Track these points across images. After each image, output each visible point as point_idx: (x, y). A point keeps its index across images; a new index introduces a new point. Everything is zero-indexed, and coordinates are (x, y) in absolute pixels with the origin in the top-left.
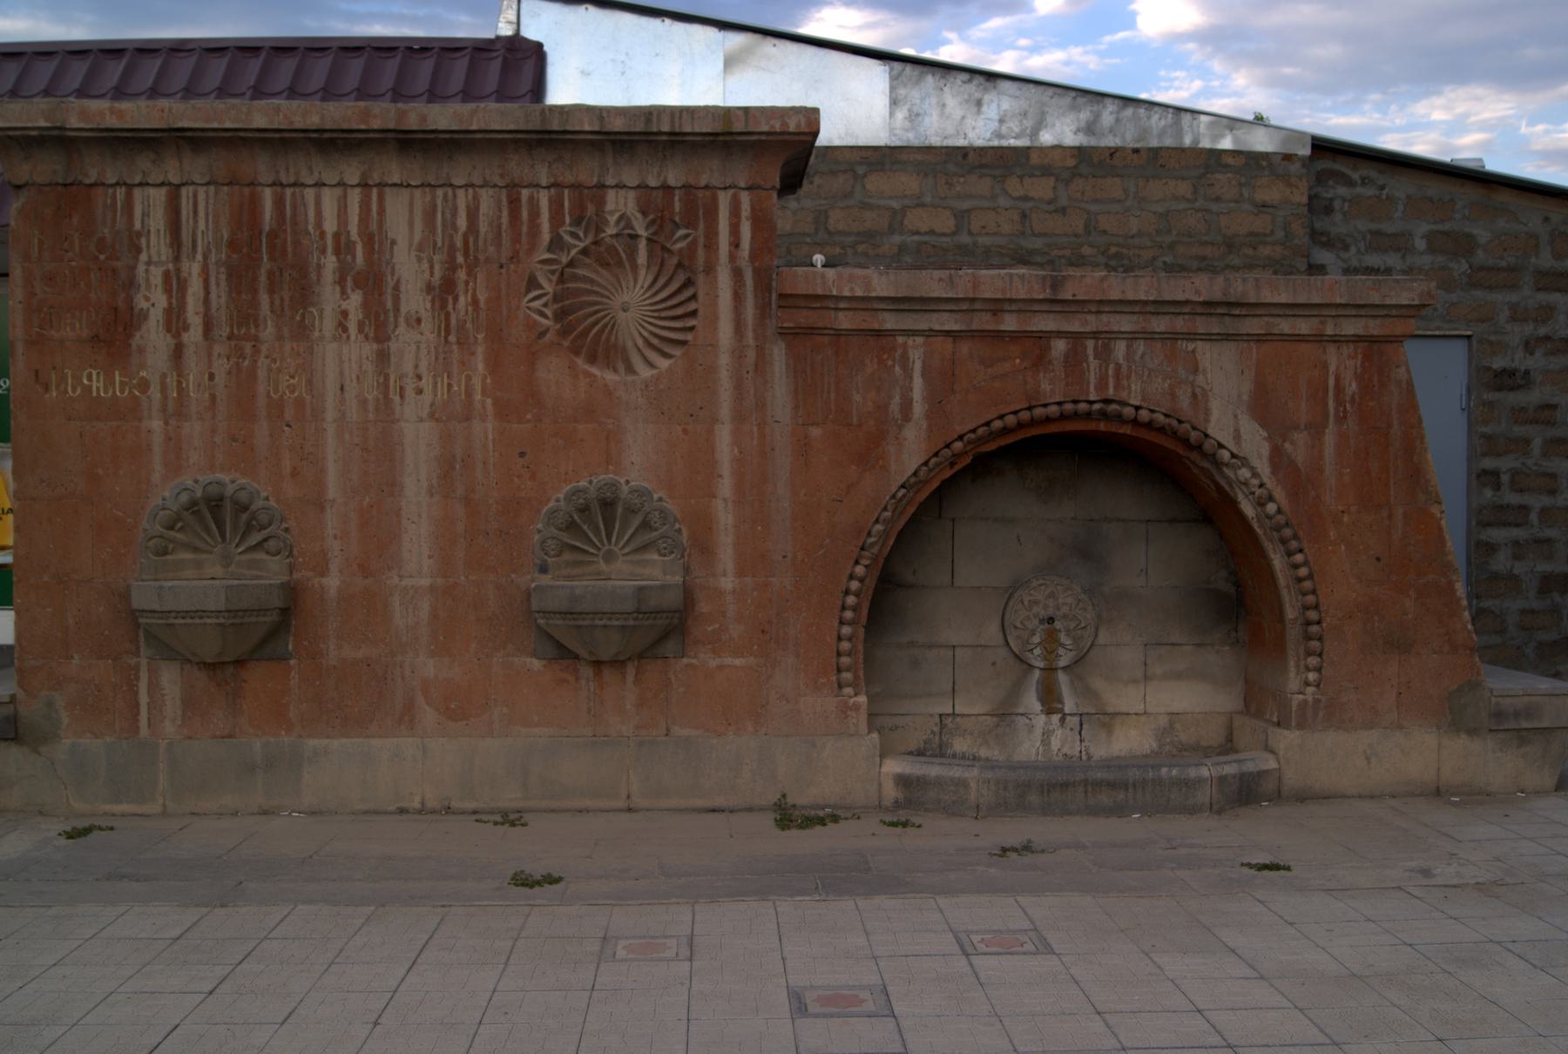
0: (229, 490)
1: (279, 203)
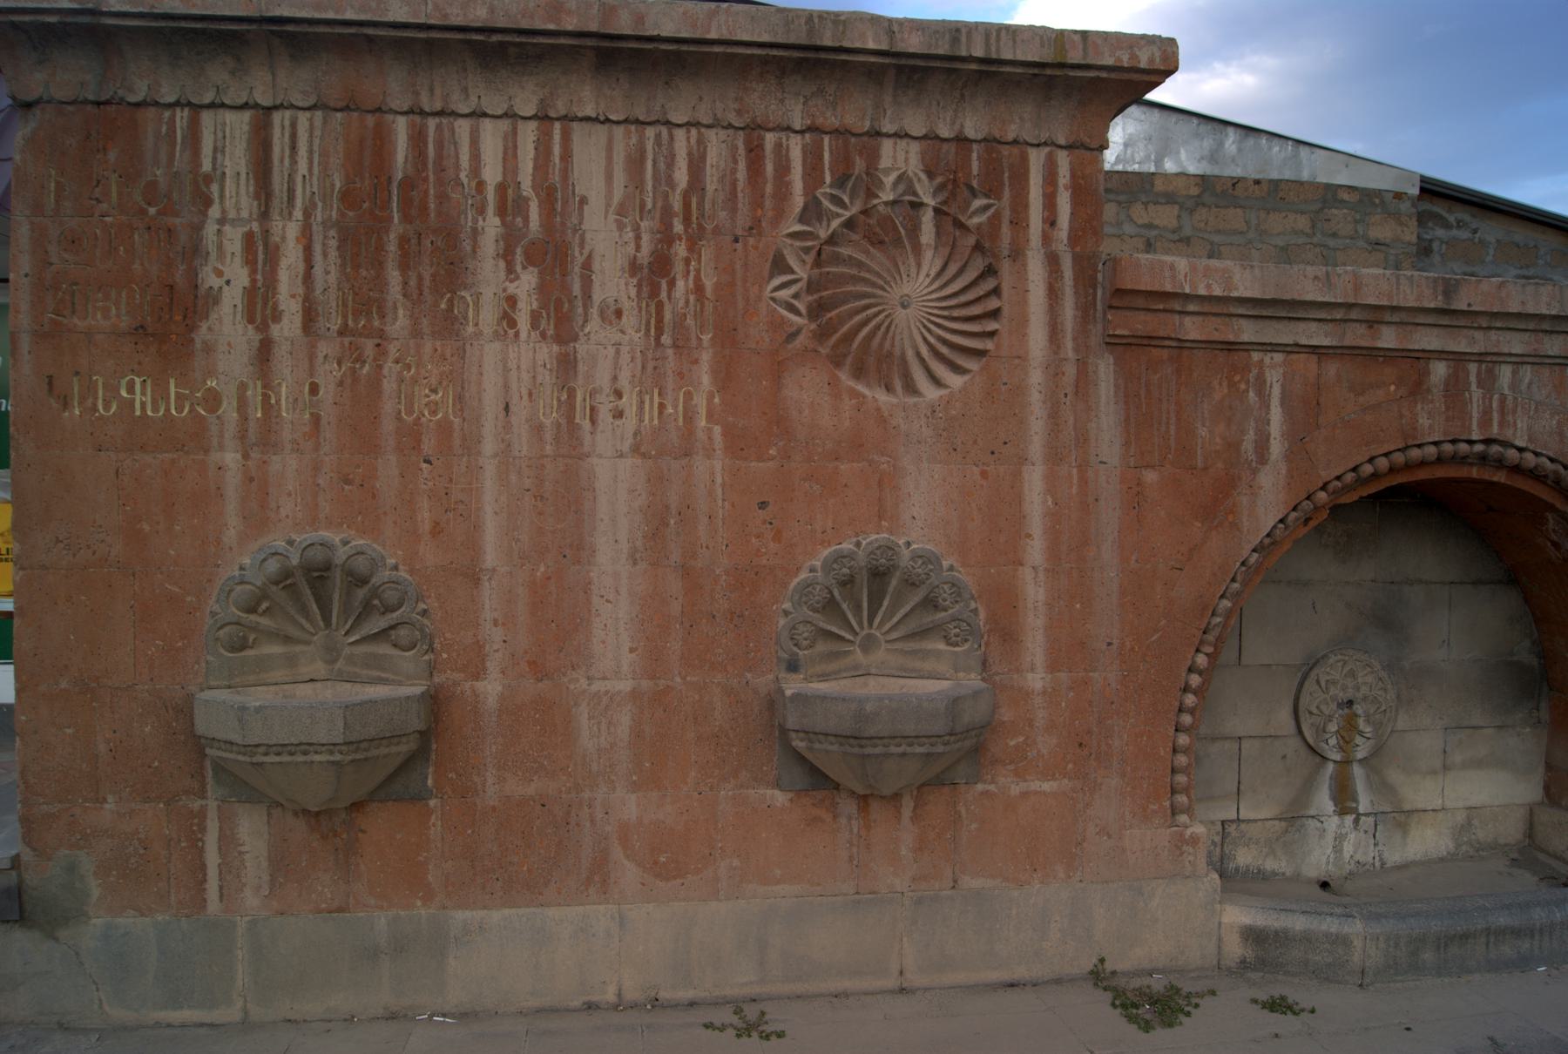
0: (341, 555)
1: (418, 139)
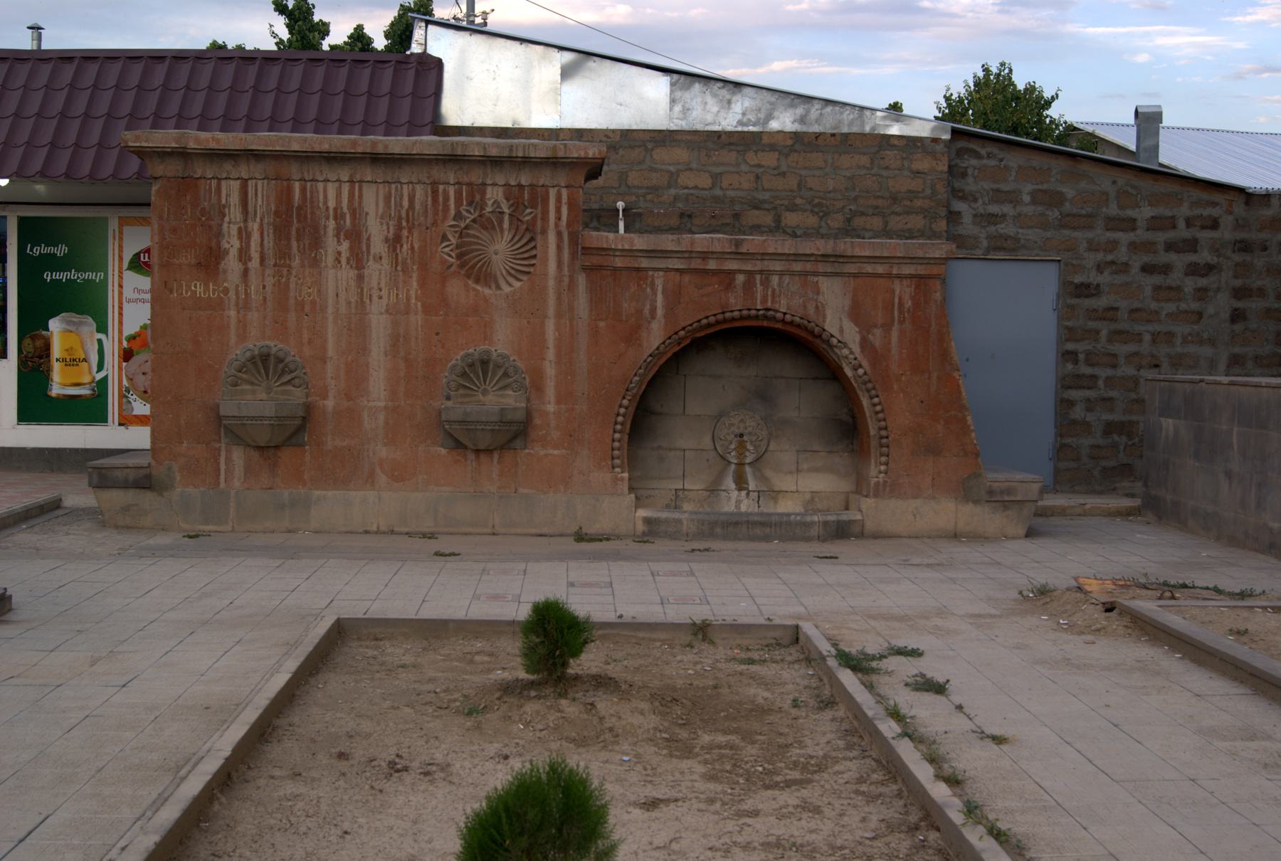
0: (274, 350)
1: (303, 190)
